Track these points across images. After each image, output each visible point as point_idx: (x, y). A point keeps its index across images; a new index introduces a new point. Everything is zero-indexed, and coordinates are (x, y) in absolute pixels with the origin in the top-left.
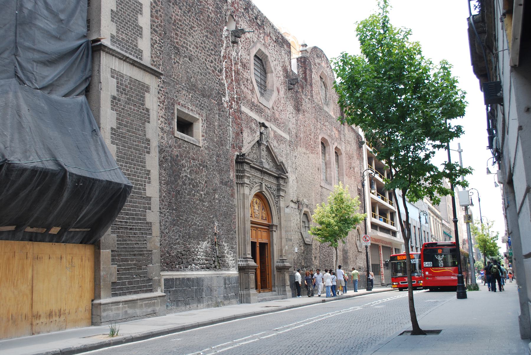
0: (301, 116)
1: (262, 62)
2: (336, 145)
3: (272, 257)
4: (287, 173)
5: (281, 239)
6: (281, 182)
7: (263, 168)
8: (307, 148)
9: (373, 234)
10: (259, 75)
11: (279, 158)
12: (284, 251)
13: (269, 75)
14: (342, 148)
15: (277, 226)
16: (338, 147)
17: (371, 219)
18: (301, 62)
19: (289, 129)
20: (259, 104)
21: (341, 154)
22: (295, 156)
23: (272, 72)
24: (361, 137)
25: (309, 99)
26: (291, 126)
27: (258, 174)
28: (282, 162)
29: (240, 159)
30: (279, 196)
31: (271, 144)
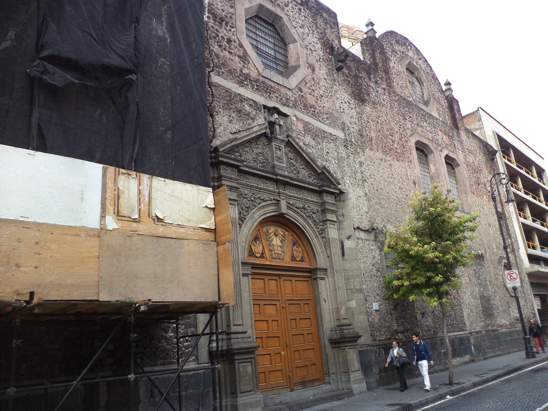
0: (368, 108)
2: (445, 152)
3: (320, 323)
4: (339, 184)
5: (336, 290)
6: (329, 199)
7: (277, 175)
8: (385, 153)
9: (532, 270)
10: (272, 46)
11: (319, 162)
12: (343, 312)
13: (291, 47)
14: (459, 157)
15: (326, 270)
16: (451, 155)
17: (527, 251)
18: (366, 45)
19: (343, 123)
20: (261, 79)
21: (458, 165)
22: (361, 163)
23: (295, 41)
24: (491, 147)
25: (384, 89)
26: (346, 118)
27: (271, 187)
28: (324, 167)
31: (297, 140)
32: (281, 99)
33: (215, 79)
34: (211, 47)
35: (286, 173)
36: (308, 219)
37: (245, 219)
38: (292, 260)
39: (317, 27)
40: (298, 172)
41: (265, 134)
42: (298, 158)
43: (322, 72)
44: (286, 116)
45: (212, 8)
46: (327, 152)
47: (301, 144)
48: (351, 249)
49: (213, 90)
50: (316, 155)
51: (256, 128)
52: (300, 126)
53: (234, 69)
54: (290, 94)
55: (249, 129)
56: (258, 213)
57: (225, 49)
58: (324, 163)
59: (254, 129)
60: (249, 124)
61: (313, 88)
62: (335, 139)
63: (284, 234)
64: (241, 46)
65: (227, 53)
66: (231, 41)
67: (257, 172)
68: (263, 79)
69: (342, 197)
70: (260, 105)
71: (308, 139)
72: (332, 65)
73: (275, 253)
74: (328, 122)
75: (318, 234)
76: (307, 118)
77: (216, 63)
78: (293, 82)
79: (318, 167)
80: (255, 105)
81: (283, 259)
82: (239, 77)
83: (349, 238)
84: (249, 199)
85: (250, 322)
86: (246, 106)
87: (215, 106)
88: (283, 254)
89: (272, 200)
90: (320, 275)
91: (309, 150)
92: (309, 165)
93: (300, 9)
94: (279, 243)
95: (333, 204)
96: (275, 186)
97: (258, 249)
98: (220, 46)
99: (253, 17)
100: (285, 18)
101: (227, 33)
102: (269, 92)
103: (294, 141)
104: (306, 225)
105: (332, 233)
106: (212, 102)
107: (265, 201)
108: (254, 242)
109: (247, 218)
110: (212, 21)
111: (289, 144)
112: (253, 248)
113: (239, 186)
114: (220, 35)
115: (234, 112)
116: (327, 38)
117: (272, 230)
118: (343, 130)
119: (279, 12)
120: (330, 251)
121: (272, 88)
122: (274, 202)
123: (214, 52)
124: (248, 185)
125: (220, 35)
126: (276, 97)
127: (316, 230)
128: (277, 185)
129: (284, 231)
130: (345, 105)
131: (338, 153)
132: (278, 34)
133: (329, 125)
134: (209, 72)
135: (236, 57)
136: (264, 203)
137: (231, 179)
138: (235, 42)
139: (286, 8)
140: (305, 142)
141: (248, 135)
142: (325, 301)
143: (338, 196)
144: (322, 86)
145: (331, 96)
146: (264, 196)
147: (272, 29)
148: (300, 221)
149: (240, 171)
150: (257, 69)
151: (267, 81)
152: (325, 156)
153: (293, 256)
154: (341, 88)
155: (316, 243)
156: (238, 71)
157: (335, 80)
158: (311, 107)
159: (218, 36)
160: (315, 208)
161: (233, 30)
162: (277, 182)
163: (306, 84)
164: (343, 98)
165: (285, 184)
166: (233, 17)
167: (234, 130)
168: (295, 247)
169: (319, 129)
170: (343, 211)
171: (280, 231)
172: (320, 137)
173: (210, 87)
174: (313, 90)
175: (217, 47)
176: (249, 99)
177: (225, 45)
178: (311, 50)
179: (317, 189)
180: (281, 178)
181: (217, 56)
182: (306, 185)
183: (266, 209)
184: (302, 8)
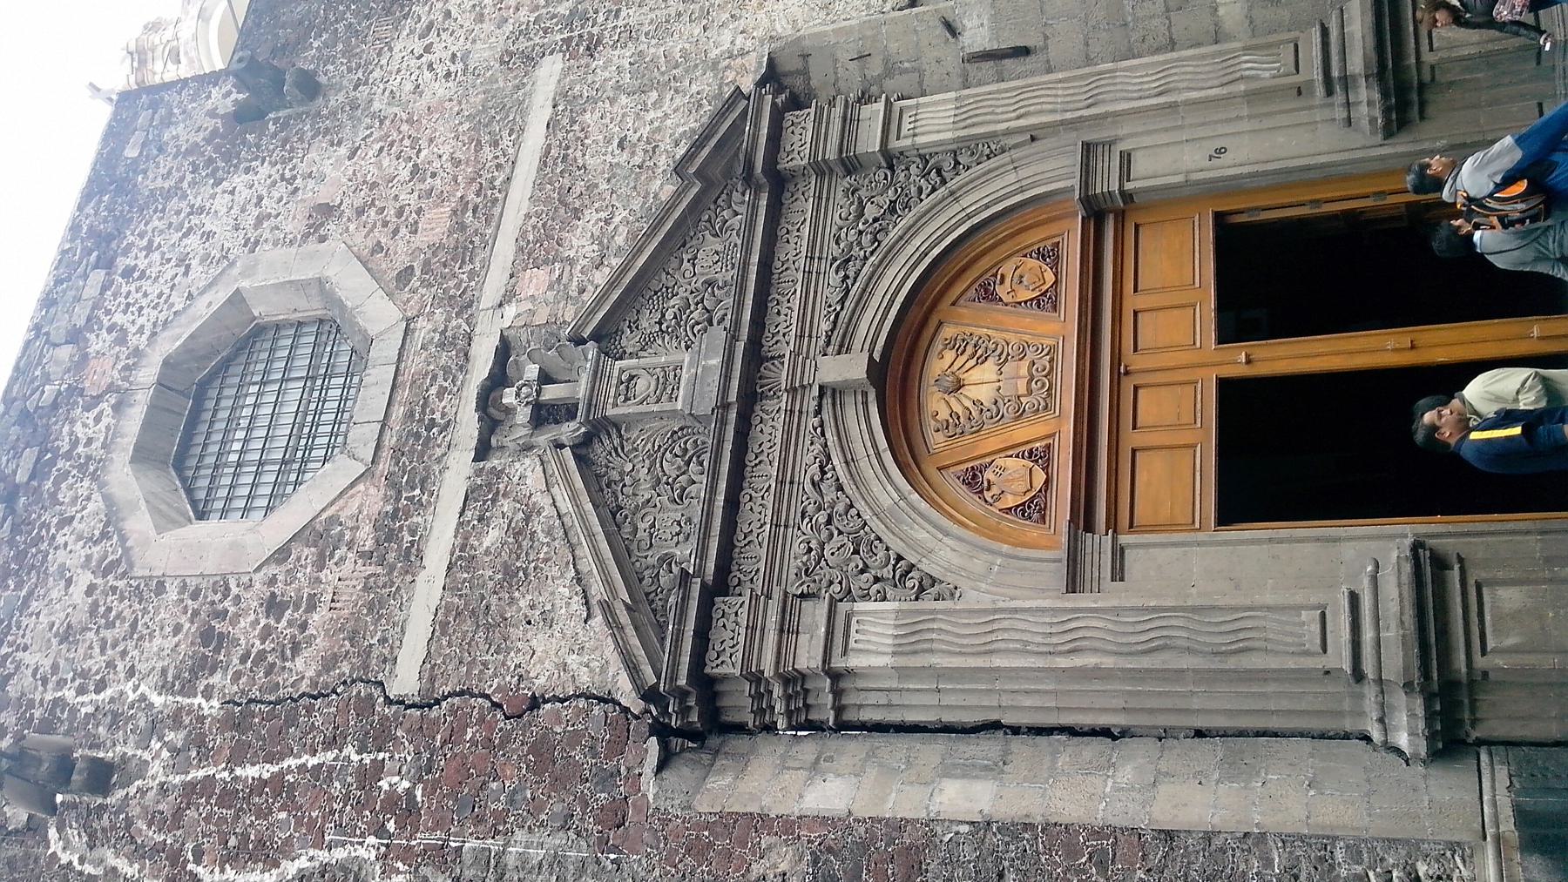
1: (203, 386)
5: (1173, 106)
7: (725, 406)
23: (237, 299)
27: (770, 429)
28: (679, 169)
29: (684, 711)
30: (891, 160)
31: (589, 297)
32: (446, 370)
33: (405, 680)
34: (304, 687)
35: (716, 361)
36: (887, 241)
37: (899, 558)
38: (1055, 308)
39: (176, 191)
40: (710, 283)
41: (582, 450)
42: (655, 285)
43: (330, 170)
44: (504, 350)
45: (176, 677)
46: (621, 145)
47: (601, 277)
48: (995, 18)
49: (447, 689)
50: (636, 204)
51: (558, 498)
52: (536, 281)
53: (366, 588)
54: (423, 328)
55: (566, 533)
56: (876, 488)
57: (304, 626)
58: (663, 162)
59: (563, 511)
60: (549, 533)
61: (391, 213)
62: (568, 105)
63: (951, 344)
64: (281, 555)
65: (316, 617)
66: (273, 595)
67: (721, 498)
68: (386, 453)
69: (789, 64)
70: (478, 473)
71: (580, 242)
72: (299, 115)
73: (1030, 392)
74: (506, 142)
75: (941, 191)
76: (504, 251)
77: (352, 670)
78: (378, 313)
79: (678, 195)
80: (481, 495)
81: (1052, 350)
82: (392, 568)
83: (952, 29)
84: (824, 534)
85: (1309, 548)
86: (487, 542)
87: (499, 689)
88: (1030, 356)
89: (822, 425)
90: (1108, 182)
91: (620, 240)
92: (676, 236)
93: (128, 273)
94: (988, 370)
95: (818, 120)
96: (770, 405)
97: (1013, 478)
98: (296, 648)
99: (183, 480)
100: (168, 344)
101: (246, 612)
102: (429, 429)
103: (592, 312)
104: (910, 249)
105: (934, 121)
106: (487, 697)
107: (829, 458)
108: (988, 495)
109: (897, 546)
110: (216, 679)
111: (605, 337)
112: (1010, 501)
113: (777, 593)
114: (258, 645)
115: (512, 601)
116: (208, 141)
117: (936, 405)
118: (530, 60)
119: (148, 374)
120: (1008, 133)
121: (410, 415)
122: (827, 415)
123: (319, 674)
124: (773, 538)
125: (258, 645)
126: (441, 393)
127: (927, 202)
128: (763, 396)
129: (938, 345)
130: (439, 52)
131: (618, 87)
132: (226, 364)
133: (518, 131)
134: (389, 702)
135: (322, 575)
136: (837, 460)
137: (754, 628)
138: (272, 581)
139: (133, 340)
140: (596, 250)
141: (591, 536)
142: (1221, 151)
143: (787, 81)
144: (380, 168)
145: (410, 121)
146: (808, 457)
147: (213, 393)
148: (897, 280)
149: (721, 585)
150: (352, 485)
151: (390, 440)
152: (637, 160)
153: (1038, 302)
154: (377, 74)
155: (984, 193)
156: (371, 569)
157: (354, 106)
158: (462, 227)
159: (262, 655)
160: (840, 208)
161: (235, 590)
162: (751, 398)
163: (378, 247)
164: (413, 63)
165: (756, 356)
166: (192, 583)
167: (577, 604)
168: (1001, 291)
169: (539, 185)
170: (844, 56)
171: (940, 363)
172: (566, 182)
173: (438, 702)
174: (400, 213)
175: (299, 663)
176: (460, 524)
177: (290, 624)
178: (259, 221)
179: (764, 202)
180: (735, 383)
181: (329, 663)
182: (755, 258)
183: (858, 447)
184: (122, 263)
